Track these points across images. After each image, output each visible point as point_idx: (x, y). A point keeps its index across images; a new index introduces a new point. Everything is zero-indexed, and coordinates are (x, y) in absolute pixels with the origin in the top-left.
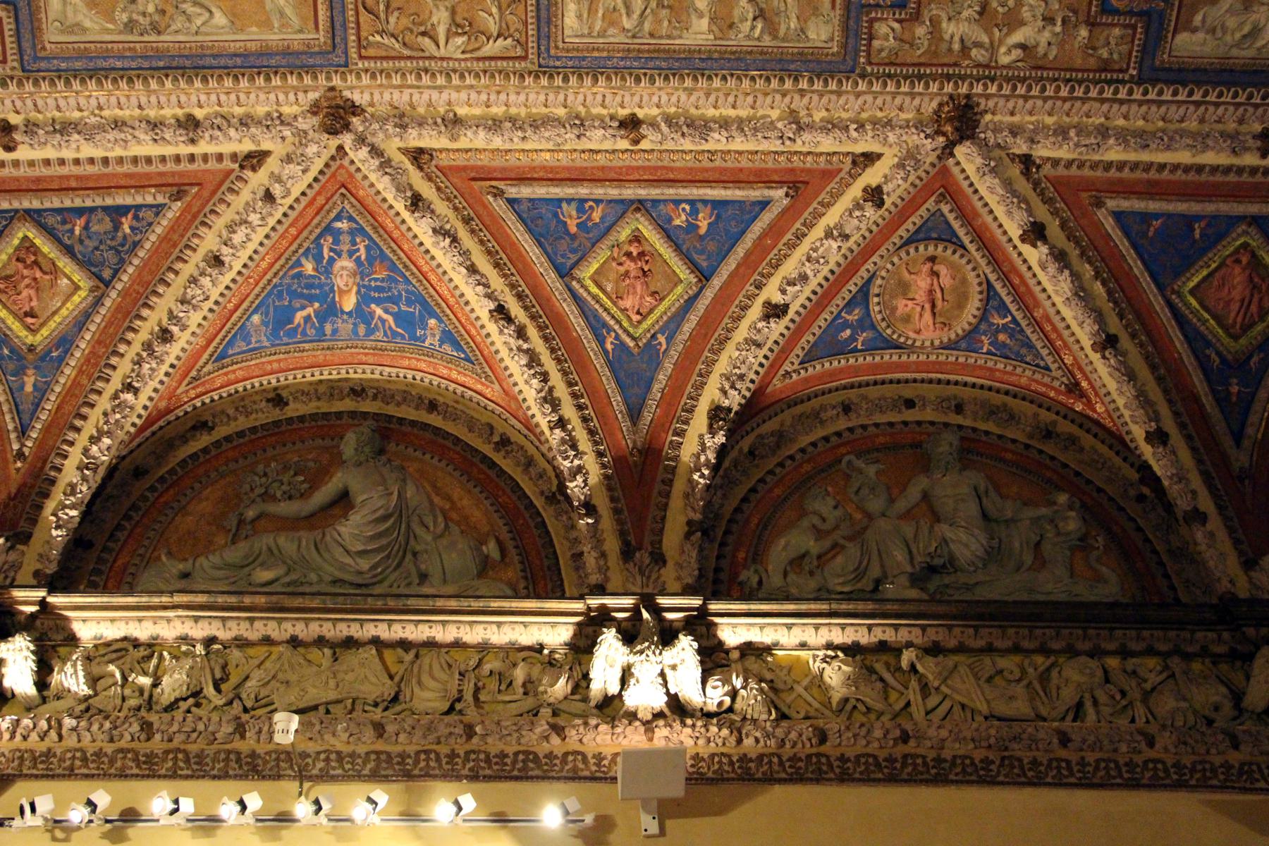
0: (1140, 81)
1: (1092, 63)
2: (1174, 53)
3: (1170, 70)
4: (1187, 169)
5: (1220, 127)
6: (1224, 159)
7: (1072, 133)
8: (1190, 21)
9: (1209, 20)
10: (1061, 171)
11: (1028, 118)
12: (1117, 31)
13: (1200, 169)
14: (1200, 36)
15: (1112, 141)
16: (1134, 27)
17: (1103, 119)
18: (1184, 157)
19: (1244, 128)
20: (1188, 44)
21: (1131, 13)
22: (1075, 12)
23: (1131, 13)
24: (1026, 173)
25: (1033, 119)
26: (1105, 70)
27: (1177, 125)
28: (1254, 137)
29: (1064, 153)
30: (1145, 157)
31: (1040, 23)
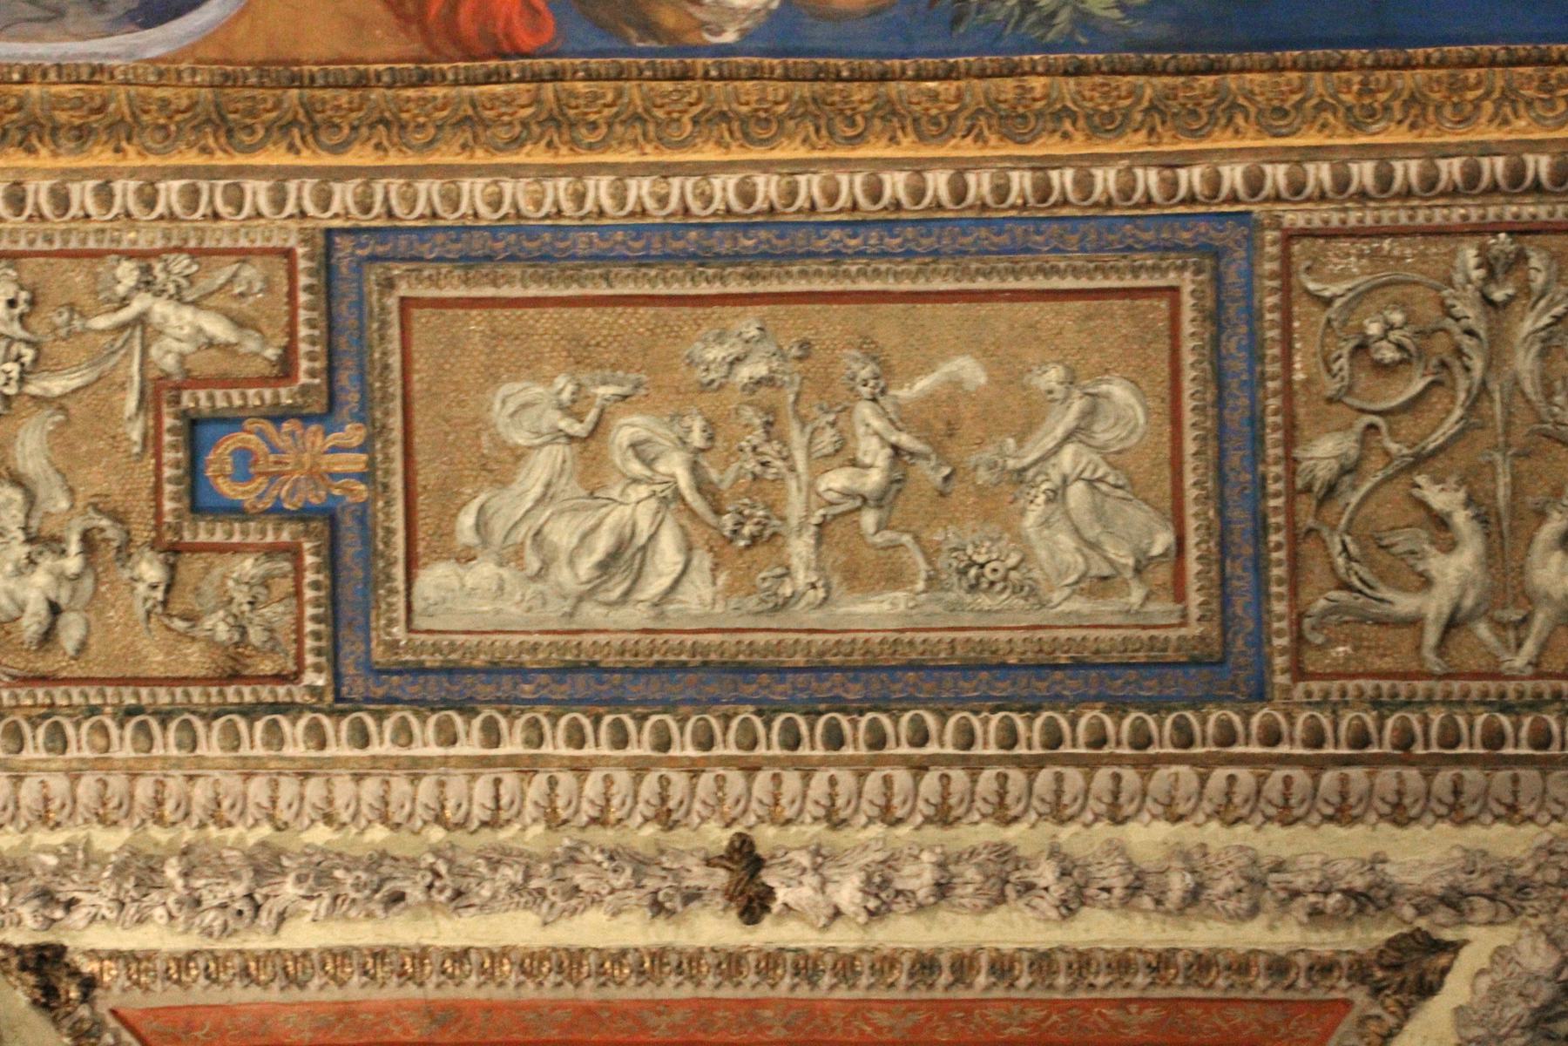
0: (340, 702)
1: (195, 659)
2: (421, 622)
3: (420, 670)
4: (531, 963)
5: (607, 837)
6: (635, 931)
7: (172, 871)
8: (446, 532)
9: (498, 527)
10: (164, 996)
11: (41, 837)
12: (248, 566)
13: (570, 961)
14: (484, 571)
15: (289, 889)
16: (293, 552)
17: (265, 830)
18: (520, 929)
19: (679, 838)
20: (461, 596)
21: (277, 512)
22: (118, 517)
23: (277, 512)
24: (47, 999)
25: (58, 838)
26: (235, 677)
27: (486, 837)
28: (708, 862)
29: (158, 935)
30: (401, 931)
31: (20, 551)
